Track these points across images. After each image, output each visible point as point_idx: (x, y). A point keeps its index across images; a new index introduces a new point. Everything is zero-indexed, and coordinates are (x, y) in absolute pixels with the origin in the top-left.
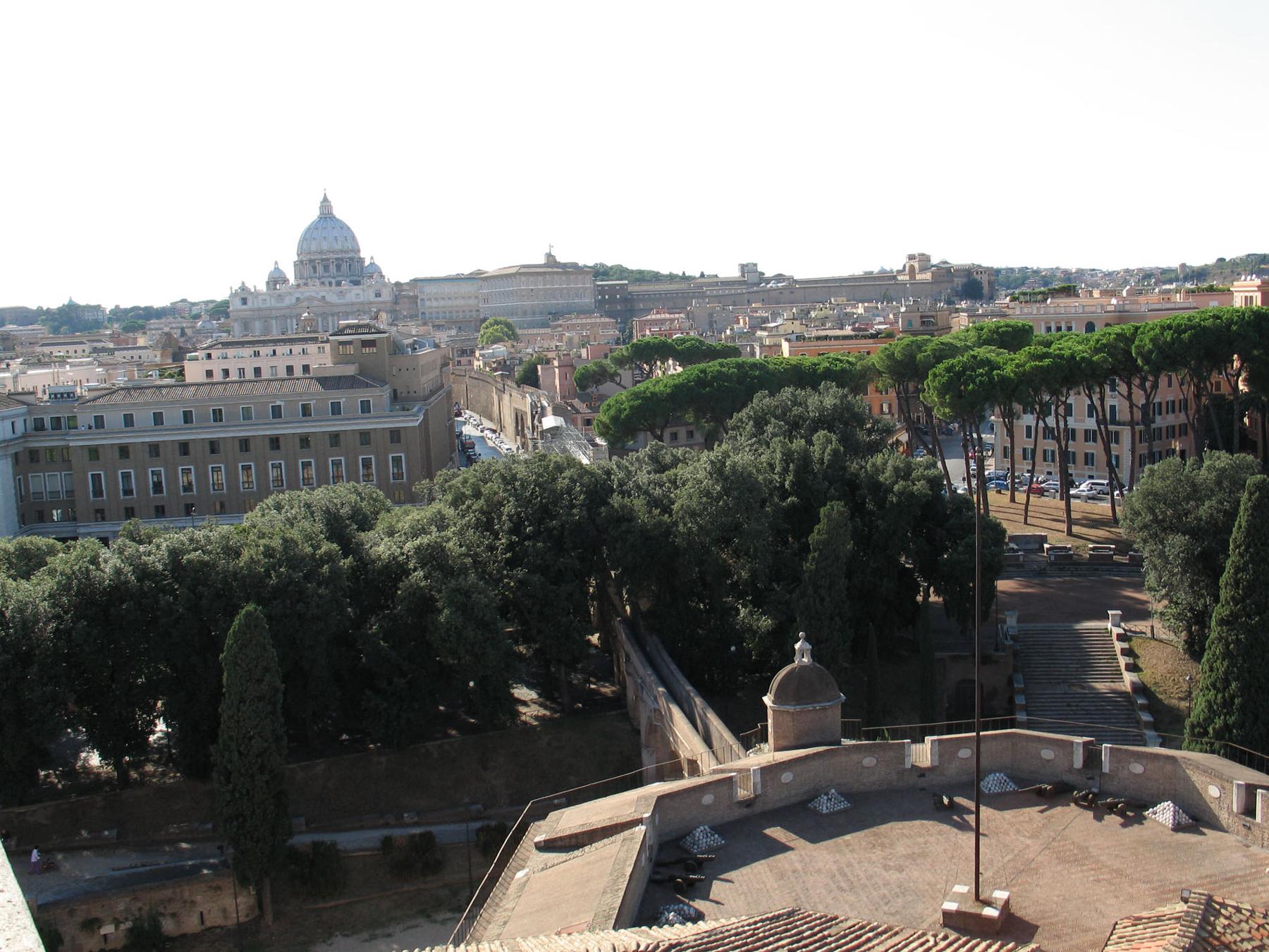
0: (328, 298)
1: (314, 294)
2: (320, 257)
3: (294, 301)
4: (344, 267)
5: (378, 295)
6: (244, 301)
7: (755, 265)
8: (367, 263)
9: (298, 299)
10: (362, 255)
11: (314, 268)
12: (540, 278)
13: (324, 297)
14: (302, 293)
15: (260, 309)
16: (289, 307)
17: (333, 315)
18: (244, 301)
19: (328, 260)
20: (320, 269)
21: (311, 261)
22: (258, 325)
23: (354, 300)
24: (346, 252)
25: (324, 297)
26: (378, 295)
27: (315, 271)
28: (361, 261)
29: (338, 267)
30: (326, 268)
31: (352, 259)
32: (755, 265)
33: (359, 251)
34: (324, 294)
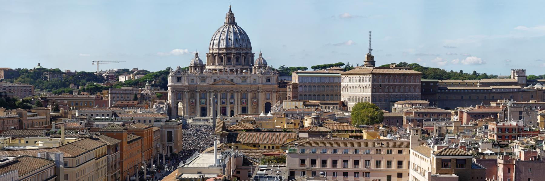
0: (235, 81)
1: (226, 77)
2: (224, 51)
3: (212, 81)
4: (242, 59)
5: (268, 80)
6: (179, 79)
7: (524, 71)
8: (256, 57)
9: (215, 80)
10: (252, 52)
11: (221, 58)
12: (386, 77)
13: (232, 80)
14: (218, 77)
15: (189, 86)
16: (210, 85)
17: (238, 92)
18: (179, 79)
19: (230, 54)
20: (225, 59)
21: (219, 54)
22: (187, 96)
23: (252, 82)
24: (243, 49)
25: (232, 80)
26: (268, 80)
27: (222, 62)
28: (253, 55)
29: (237, 59)
30: (229, 59)
31: (246, 54)
32: (524, 71)
33: (251, 49)
34: (232, 78)
